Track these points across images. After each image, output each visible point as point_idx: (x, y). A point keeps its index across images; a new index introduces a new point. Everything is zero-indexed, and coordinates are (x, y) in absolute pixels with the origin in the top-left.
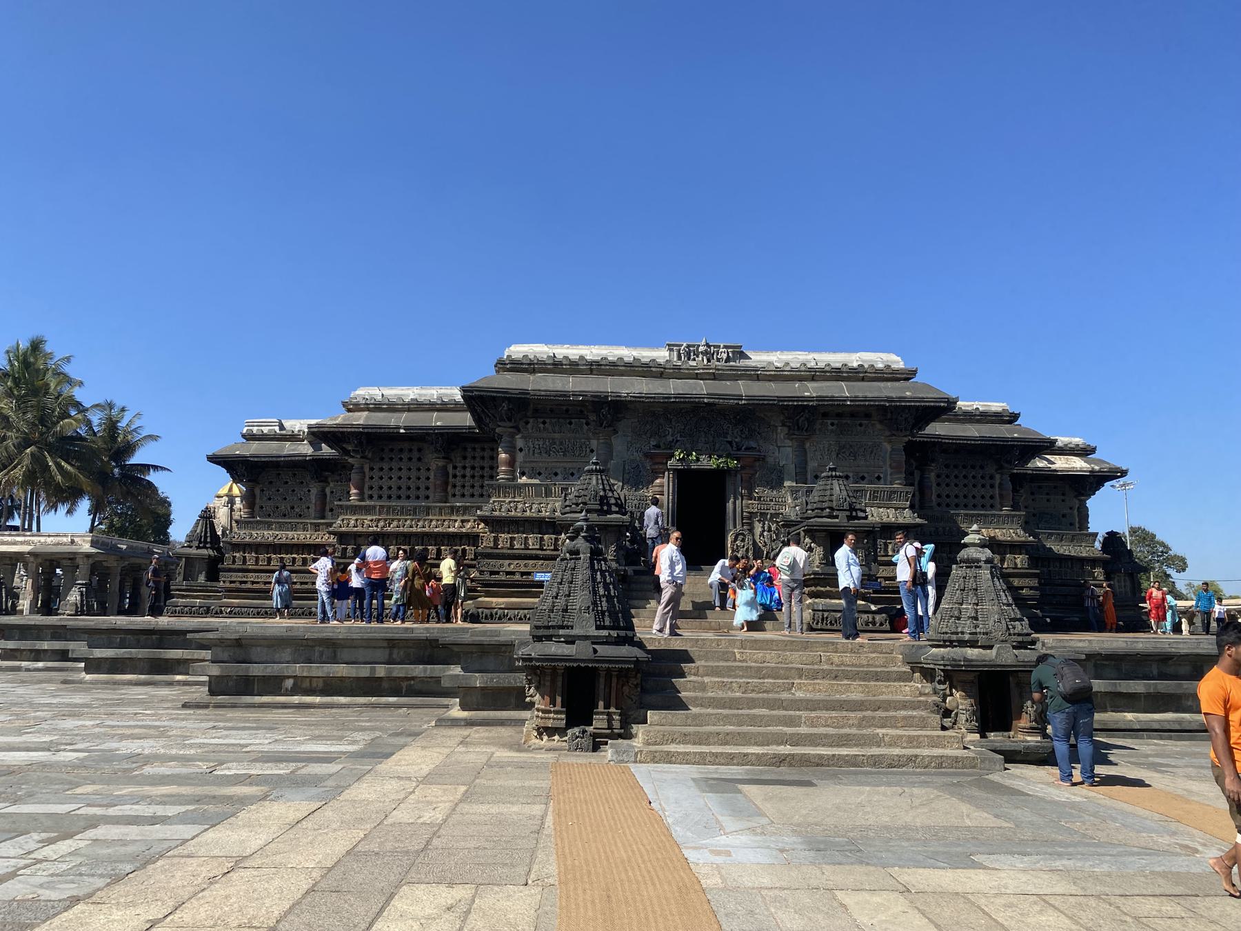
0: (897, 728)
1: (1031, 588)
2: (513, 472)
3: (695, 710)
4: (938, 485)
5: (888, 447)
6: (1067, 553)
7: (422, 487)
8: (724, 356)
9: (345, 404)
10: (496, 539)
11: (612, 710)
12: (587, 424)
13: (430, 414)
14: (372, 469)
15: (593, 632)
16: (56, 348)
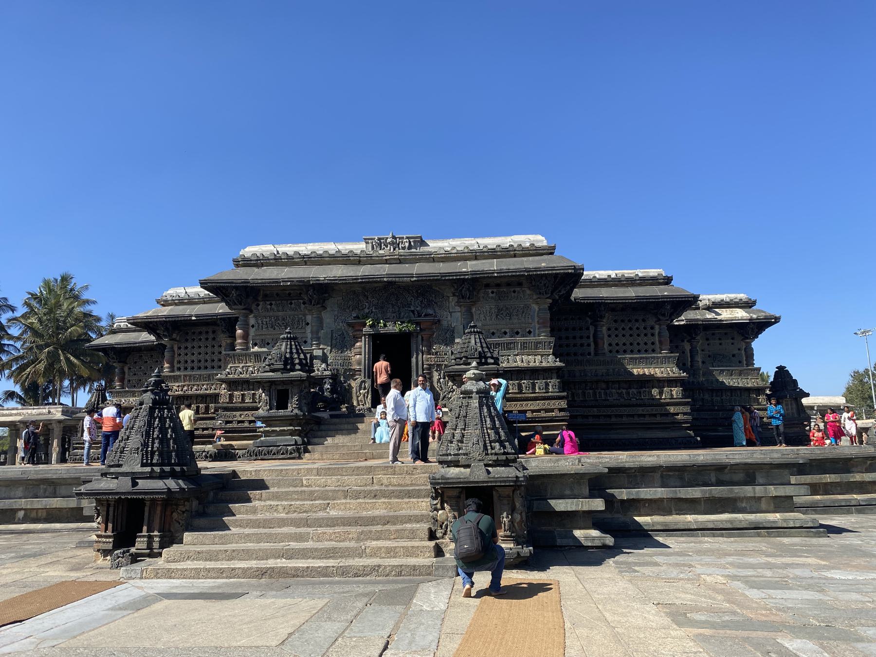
0: (390, 539)
1: (685, 414)
2: (247, 343)
3: (234, 530)
4: (609, 336)
5: (535, 307)
6: (736, 385)
7: (216, 359)
8: (407, 245)
9: (158, 302)
10: (231, 396)
11: (156, 533)
12: (304, 303)
13: (216, 305)
14: (179, 348)
15: (138, 469)
16: (77, 283)
